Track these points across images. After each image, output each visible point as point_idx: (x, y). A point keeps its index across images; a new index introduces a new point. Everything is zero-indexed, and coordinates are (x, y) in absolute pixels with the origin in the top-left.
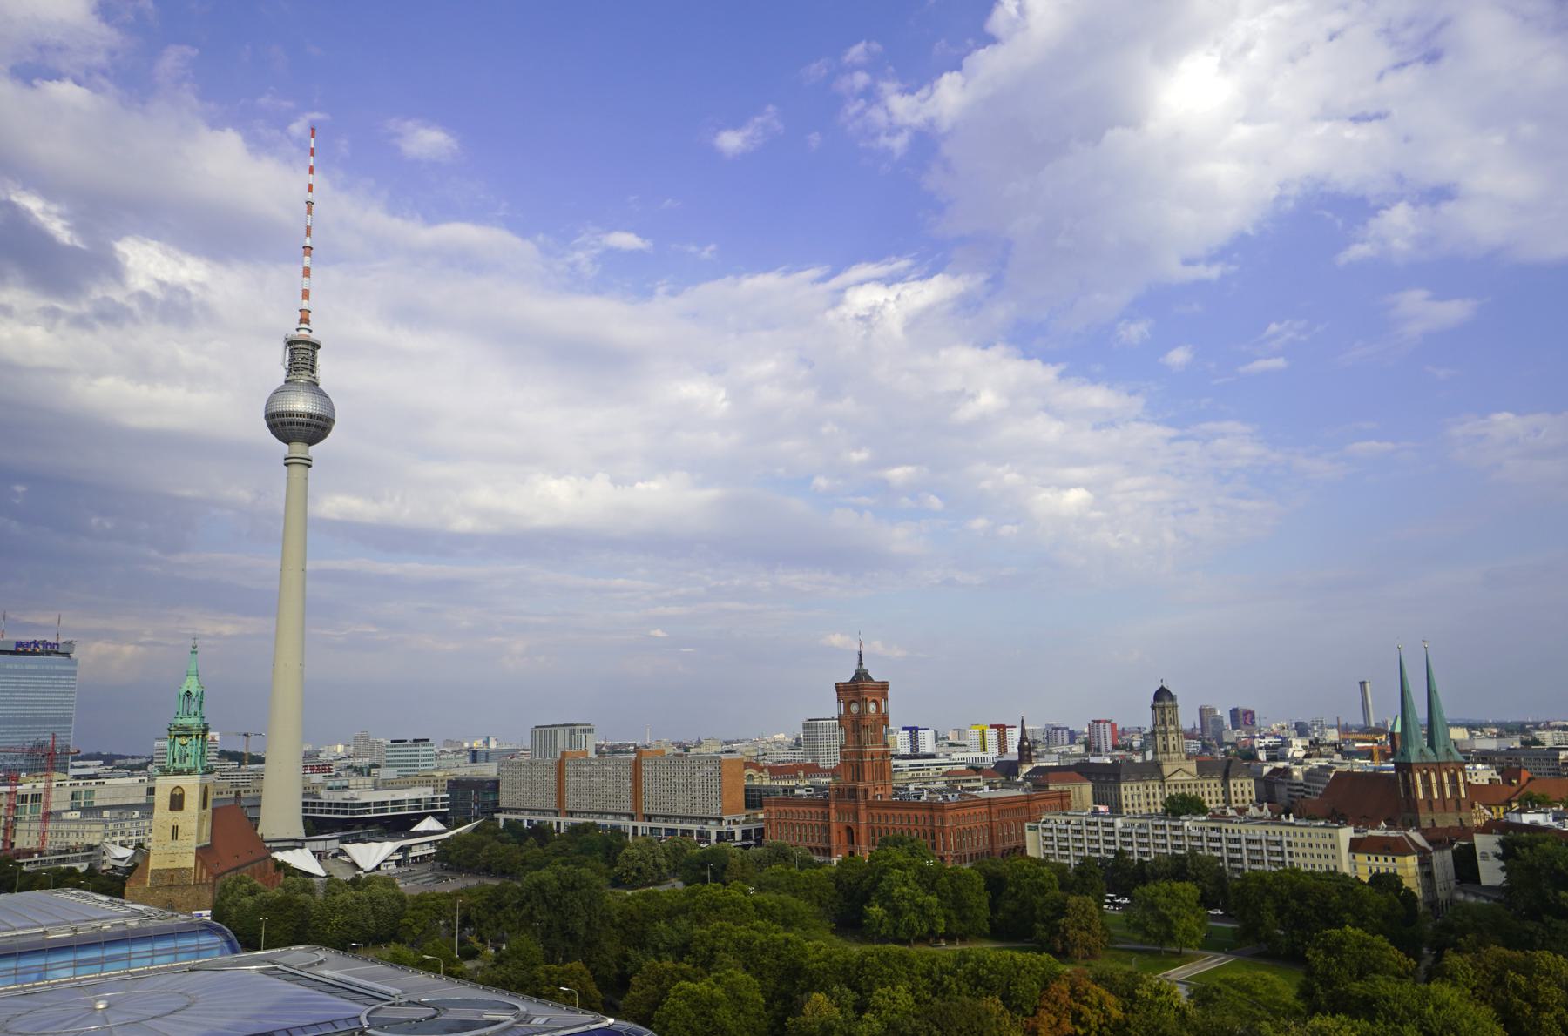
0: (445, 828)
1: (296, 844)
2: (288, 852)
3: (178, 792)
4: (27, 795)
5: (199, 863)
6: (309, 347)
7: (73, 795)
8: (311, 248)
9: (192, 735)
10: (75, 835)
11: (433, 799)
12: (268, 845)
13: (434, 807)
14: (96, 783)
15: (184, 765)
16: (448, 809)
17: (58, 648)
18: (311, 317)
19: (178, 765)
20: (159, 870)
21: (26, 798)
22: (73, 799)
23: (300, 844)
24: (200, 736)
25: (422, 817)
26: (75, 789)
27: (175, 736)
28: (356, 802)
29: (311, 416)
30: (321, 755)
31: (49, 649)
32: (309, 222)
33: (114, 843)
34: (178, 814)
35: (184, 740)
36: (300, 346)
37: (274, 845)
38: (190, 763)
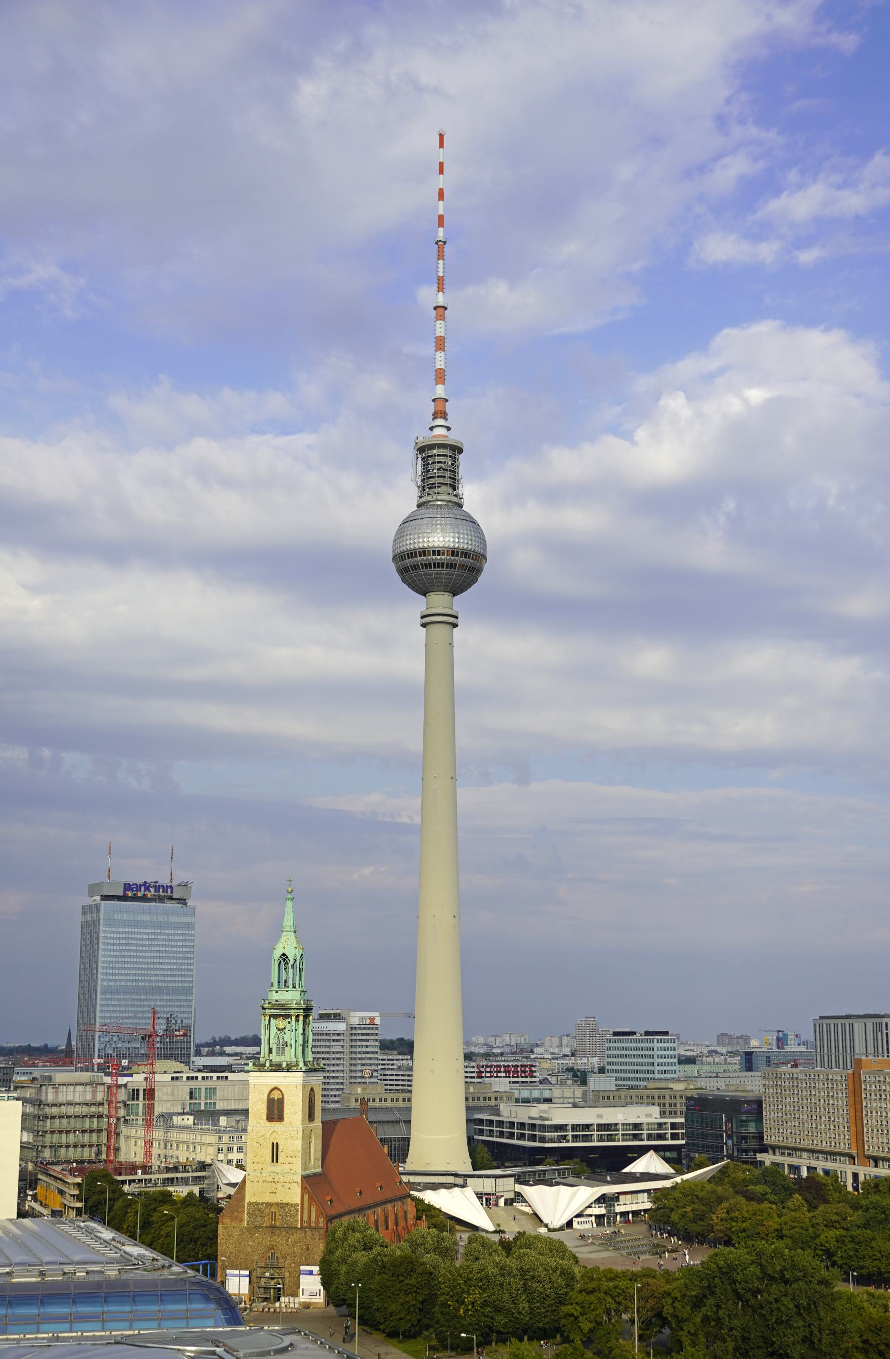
0: (673, 1171)
1: (458, 1180)
2: (443, 1191)
3: (276, 1095)
4: (138, 1090)
5: (306, 1197)
6: (447, 452)
7: (191, 1093)
8: (446, 308)
9: (290, 1016)
10: (185, 1146)
11: (660, 1125)
12: (405, 1179)
13: (661, 1137)
14: (218, 1078)
15: (282, 1058)
16: (683, 1142)
17: (172, 892)
18: (449, 407)
19: (275, 1058)
20: (257, 1204)
21: (138, 1095)
22: (191, 1098)
23: (460, 1181)
24: (301, 1018)
25: (642, 1151)
26: (193, 1084)
27: (270, 1016)
28: (547, 1123)
29: (454, 552)
30: (536, 1050)
31: (161, 893)
32: (441, 270)
33: (230, 1162)
34: (277, 1126)
35: (281, 1023)
36: (435, 451)
37: (413, 1179)
38: (289, 1056)
